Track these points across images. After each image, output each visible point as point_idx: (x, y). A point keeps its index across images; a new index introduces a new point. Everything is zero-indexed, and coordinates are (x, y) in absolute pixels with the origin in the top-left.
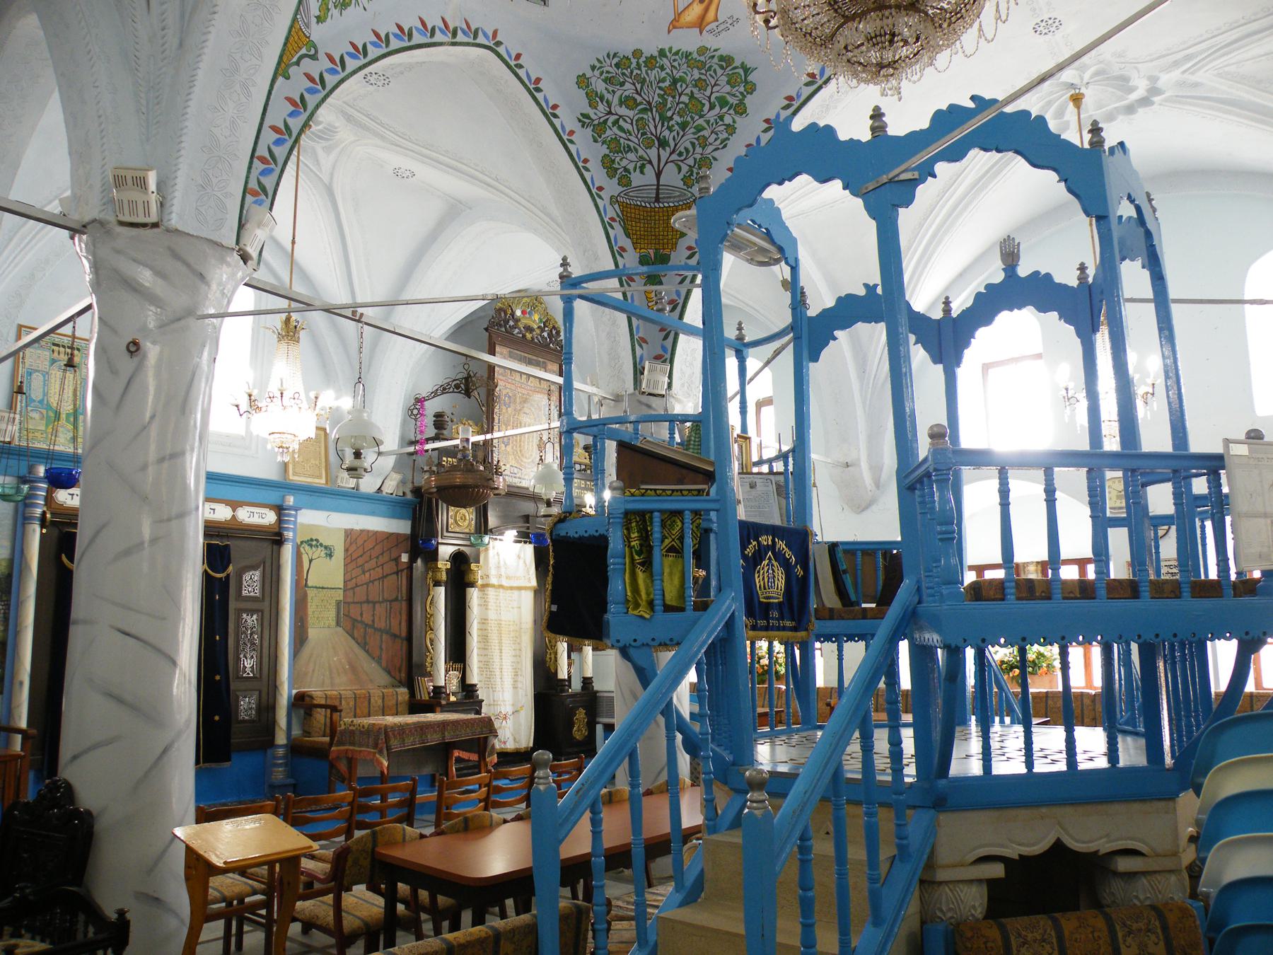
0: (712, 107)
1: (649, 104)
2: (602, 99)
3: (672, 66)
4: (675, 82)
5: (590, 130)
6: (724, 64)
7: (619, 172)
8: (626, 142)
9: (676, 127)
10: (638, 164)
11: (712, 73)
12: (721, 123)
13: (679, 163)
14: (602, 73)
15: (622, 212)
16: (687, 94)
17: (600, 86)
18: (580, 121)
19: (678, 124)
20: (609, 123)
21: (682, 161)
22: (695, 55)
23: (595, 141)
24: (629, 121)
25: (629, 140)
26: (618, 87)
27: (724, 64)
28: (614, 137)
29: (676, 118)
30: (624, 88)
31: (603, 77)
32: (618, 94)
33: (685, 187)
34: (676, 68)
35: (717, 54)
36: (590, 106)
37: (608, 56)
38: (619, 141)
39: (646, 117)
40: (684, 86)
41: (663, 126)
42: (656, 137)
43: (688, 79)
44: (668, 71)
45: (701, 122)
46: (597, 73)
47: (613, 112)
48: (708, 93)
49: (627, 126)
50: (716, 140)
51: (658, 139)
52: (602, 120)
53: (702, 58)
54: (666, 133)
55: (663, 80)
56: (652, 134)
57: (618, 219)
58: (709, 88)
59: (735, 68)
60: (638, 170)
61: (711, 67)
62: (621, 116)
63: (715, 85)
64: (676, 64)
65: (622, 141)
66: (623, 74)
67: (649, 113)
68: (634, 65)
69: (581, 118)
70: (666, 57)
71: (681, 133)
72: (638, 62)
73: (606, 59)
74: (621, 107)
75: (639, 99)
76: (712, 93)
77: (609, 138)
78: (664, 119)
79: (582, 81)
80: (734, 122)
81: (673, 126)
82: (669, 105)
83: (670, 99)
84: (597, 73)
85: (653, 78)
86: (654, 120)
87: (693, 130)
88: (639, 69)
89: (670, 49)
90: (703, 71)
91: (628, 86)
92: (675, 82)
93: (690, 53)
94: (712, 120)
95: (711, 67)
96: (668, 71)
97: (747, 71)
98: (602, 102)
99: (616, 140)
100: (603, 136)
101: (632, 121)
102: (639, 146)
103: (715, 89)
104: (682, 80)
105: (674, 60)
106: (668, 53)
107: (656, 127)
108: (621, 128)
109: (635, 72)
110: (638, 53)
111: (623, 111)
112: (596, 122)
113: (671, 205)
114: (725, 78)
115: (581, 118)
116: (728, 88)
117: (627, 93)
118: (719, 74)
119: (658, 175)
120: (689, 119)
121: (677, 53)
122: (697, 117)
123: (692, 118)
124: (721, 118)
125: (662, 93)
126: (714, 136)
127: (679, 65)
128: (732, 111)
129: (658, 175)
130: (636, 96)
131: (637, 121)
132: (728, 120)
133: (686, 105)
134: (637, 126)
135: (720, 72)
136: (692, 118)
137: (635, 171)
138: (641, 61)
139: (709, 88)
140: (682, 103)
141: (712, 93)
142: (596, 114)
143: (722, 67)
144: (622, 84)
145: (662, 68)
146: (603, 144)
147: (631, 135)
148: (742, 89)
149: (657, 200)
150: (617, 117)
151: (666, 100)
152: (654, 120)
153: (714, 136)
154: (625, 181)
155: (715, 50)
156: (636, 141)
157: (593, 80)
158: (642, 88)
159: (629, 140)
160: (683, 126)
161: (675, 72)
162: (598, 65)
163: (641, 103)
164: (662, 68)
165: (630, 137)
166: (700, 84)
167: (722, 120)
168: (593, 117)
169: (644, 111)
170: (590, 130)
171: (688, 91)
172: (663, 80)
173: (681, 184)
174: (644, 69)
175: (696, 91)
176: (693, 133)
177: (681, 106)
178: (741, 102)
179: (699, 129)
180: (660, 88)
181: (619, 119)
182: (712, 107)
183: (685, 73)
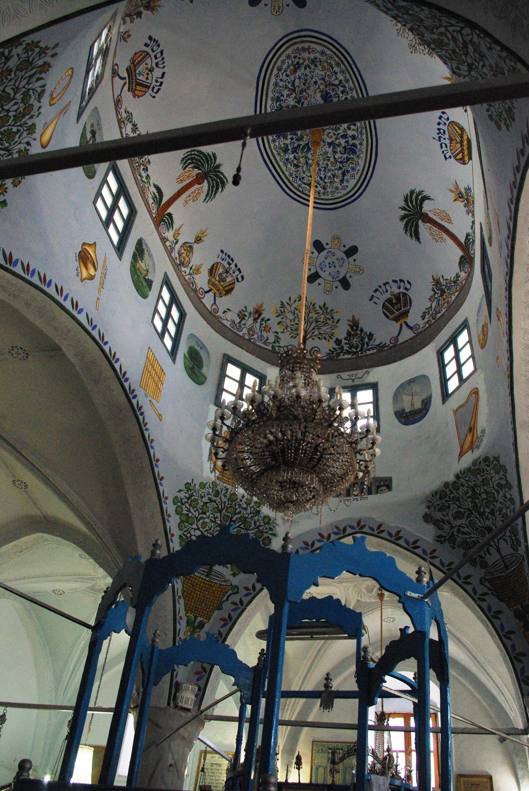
0: (498, 494)
1: (469, 509)
2: (443, 521)
3: (466, 481)
4: (473, 489)
5: (447, 543)
6: (487, 463)
7: (477, 560)
8: (472, 539)
9: (490, 516)
10: (485, 550)
11: (486, 472)
12: (507, 500)
13: (504, 537)
14: (435, 508)
15: (492, 585)
16: (483, 492)
17: (438, 515)
18: (438, 541)
19: (489, 513)
20: (456, 534)
21: (504, 535)
22: (473, 468)
23: (454, 548)
24: (466, 526)
25: (472, 537)
26: (448, 510)
27: (487, 463)
28: (462, 540)
29: (487, 510)
30: (452, 508)
31: (437, 509)
32: (450, 515)
33: (515, 552)
34: (468, 481)
35: (481, 459)
36: (439, 529)
37: (433, 495)
38: (467, 541)
39: (472, 519)
40: (479, 488)
41: (483, 519)
42: (483, 527)
43: (478, 483)
44: (466, 485)
45: (499, 505)
46: (432, 509)
47: (454, 525)
48: (491, 485)
49: (466, 530)
50: (510, 512)
51: (485, 528)
52: (450, 534)
53: (477, 467)
54: (487, 522)
55: (467, 493)
56: (481, 527)
57: (490, 592)
58: (490, 481)
59: (493, 461)
60: (487, 553)
61: (483, 469)
62: (459, 526)
63: (492, 478)
64: (467, 479)
65: (468, 540)
66: (446, 501)
67: (473, 516)
68: (448, 493)
69: (438, 539)
70: (460, 478)
71: (494, 518)
72: (449, 490)
73: (433, 498)
74: (456, 520)
75: (462, 510)
76: (493, 484)
77: (460, 542)
78: (482, 514)
79: (427, 518)
80: (511, 495)
81: (488, 516)
82: (479, 505)
83: (477, 500)
84: (432, 509)
85: (462, 495)
86: (477, 518)
87: (498, 513)
88: (452, 493)
89: (461, 471)
90: (482, 474)
91: (452, 506)
92: (473, 489)
93: (470, 468)
94: (502, 501)
95: (483, 469)
96: (466, 485)
97: (497, 459)
98: (444, 523)
99: (465, 542)
100: (456, 543)
101: (466, 525)
102: (478, 538)
103: (493, 479)
104: (475, 486)
105: (466, 477)
106: (460, 475)
107: (480, 522)
108: (464, 533)
109: (452, 496)
110: (446, 485)
111: (459, 522)
112: (448, 537)
113: (515, 567)
114: (493, 471)
115: (438, 539)
116: (497, 477)
117: (454, 511)
118: (489, 471)
119: (498, 551)
120: (493, 507)
121: (464, 472)
122: (495, 503)
123: (493, 505)
124: (505, 496)
125: (471, 499)
126: (508, 510)
127: (469, 478)
128: (507, 490)
129: (498, 551)
130: (460, 509)
131: (469, 523)
132: (509, 496)
133: (486, 499)
134: (470, 526)
135: (488, 469)
136: (493, 505)
137: (485, 555)
138: (450, 488)
139: (490, 481)
140: (484, 499)
141: (493, 484)
142: (445, 532)
143: (488, 466)
144: (449, 507)
145: (463, 485)
146: (459, 547)
147: (470, 534)
148: (502, 473)
149: (507, 567)
150: (457, 528)
151: (475, 502)
152: (477, 518)
153: (508, 510)
154: (484, 564)
155: (480, 458)
156: (475, 536)
157: (433, 514)
158: (460, 504)
159: (472, 537)
160: (492, 512)
161: (470, 483)
162: (430, 504)
163: (465, 512)
164: (463, 485)
165: (472, 536)
166: (485, 482)
167: (506, 498)
168: (444, 534)
169: (468, 517)
170: (447, 543)
171: (482, 490)
172: (467, 493)
173: (512, 551)
174: (454, 492)
175: (485, 488)
176: (500, 514)
177: (485, 501)
178: (508, 482)
179: (500, 510)
180: (469, 497)
181: (459, 529)
182: (498, 494)
183: (474, 481)
